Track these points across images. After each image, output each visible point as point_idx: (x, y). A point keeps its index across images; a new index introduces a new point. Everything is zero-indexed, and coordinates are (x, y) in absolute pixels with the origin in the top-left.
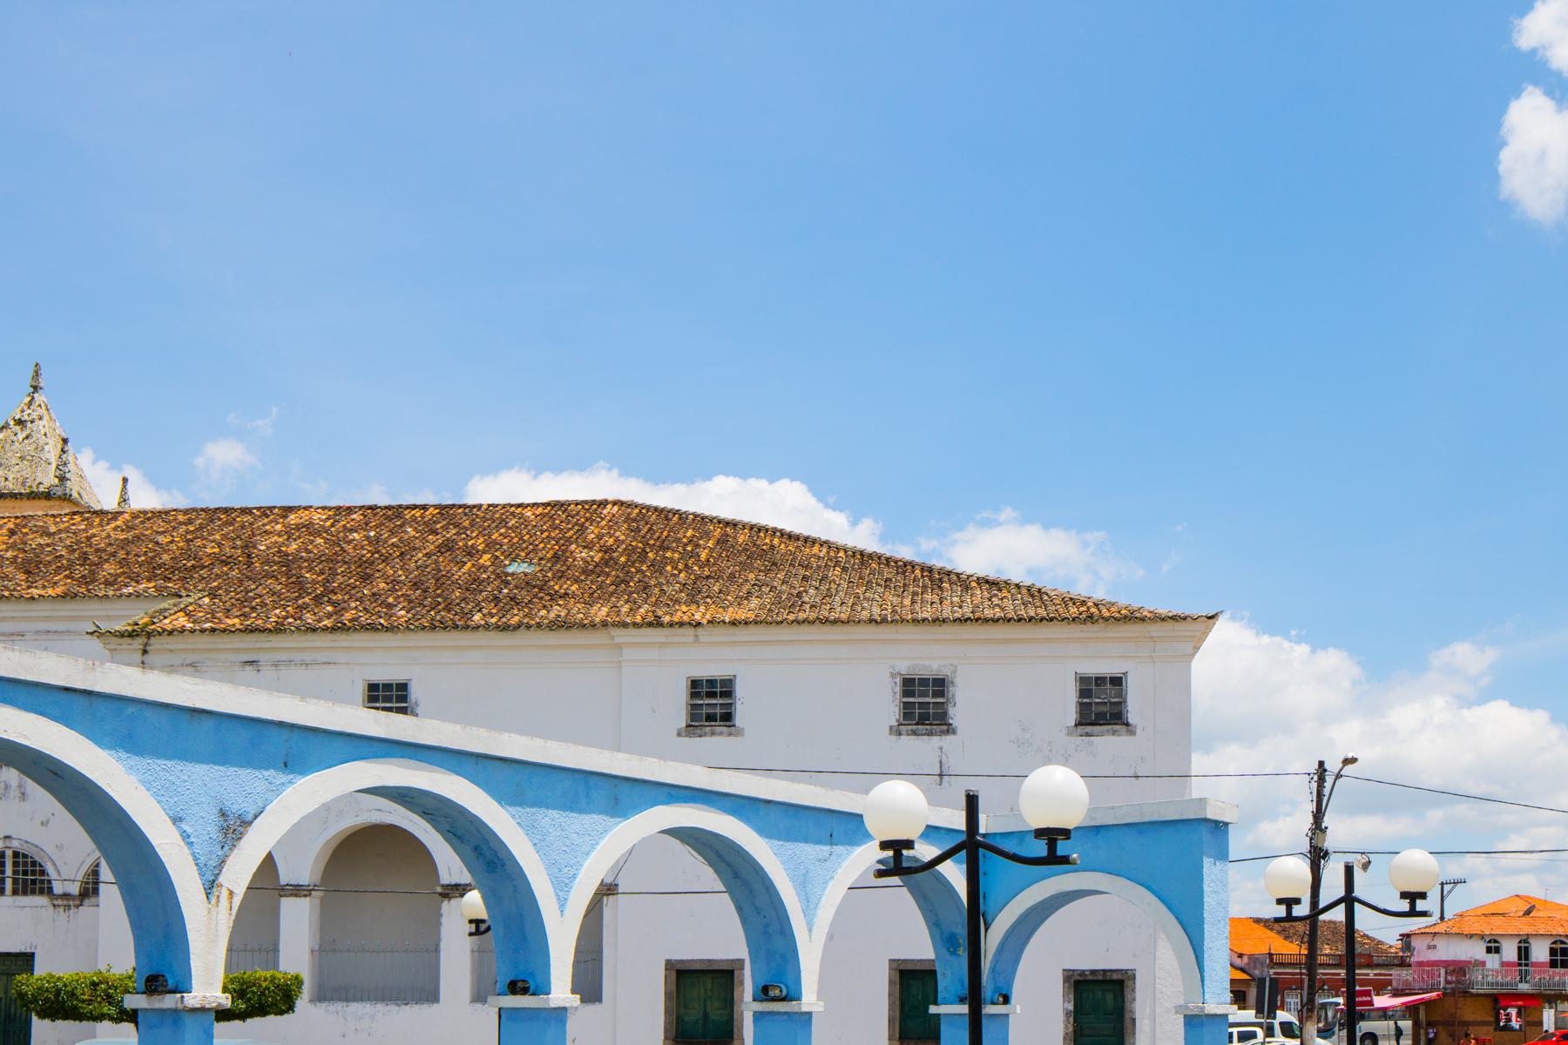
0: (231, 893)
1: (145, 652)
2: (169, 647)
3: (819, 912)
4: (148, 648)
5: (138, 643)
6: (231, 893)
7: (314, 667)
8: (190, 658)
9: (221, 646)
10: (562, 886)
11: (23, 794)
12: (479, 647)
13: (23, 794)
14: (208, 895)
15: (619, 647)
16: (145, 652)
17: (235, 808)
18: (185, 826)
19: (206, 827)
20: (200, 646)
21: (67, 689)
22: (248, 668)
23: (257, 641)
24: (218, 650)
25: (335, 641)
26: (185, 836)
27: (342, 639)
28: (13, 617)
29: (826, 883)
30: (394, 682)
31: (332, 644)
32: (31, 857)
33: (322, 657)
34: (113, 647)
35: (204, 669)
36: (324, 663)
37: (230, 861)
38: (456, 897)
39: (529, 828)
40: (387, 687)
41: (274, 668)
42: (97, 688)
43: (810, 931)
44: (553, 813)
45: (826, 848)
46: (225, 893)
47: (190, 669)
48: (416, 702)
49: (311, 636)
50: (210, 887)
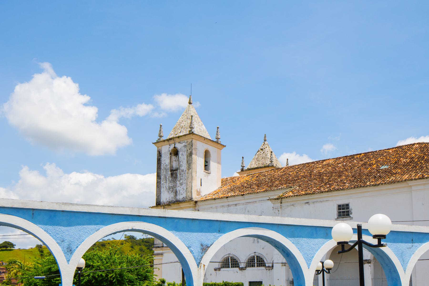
0: (204, 265)
1: (281, 203)
2: (287, 201)
3: (409, 265)
4: (282, 202)
5: (280, 200)
6: (204, 265)
7: (323, 202)
8: (292, 203)
9: (299, 199)
10: (309, 261)
11: (258, 241)
12: (368, 192)
13: (258, 241)
14: (198, 266)
15: (411, 186)
16: (281, 203)
17: (205, 243)
18: (191, 249)
19: (197, 249)
20: (294, 200)
21: (160, 217)
22: (306, 204)
23: (308, 197)
24: (299, 200)
25: (328, 194)
26: (191, 251)
27: (330, 194)
28: (254, 198)
29: (411, 255)
30: (341, 204)
31: (328, 195)
32: (261, 257)
33: (325, 199)
34: (273, 202)
35: (296, 206)
36: (326, 201)
37: (204, 257)
38: (366, 263)
39: (297, 244)
40: (343, 205)
41: (313, 204)
42: (167, 216)
43: (405, 271)
44: (305, 239)
45: (410, 245)
46: (202, 265)
47: (292, 206)
48: (351, 209)
49: (322, 194)
50: (199, 264)
